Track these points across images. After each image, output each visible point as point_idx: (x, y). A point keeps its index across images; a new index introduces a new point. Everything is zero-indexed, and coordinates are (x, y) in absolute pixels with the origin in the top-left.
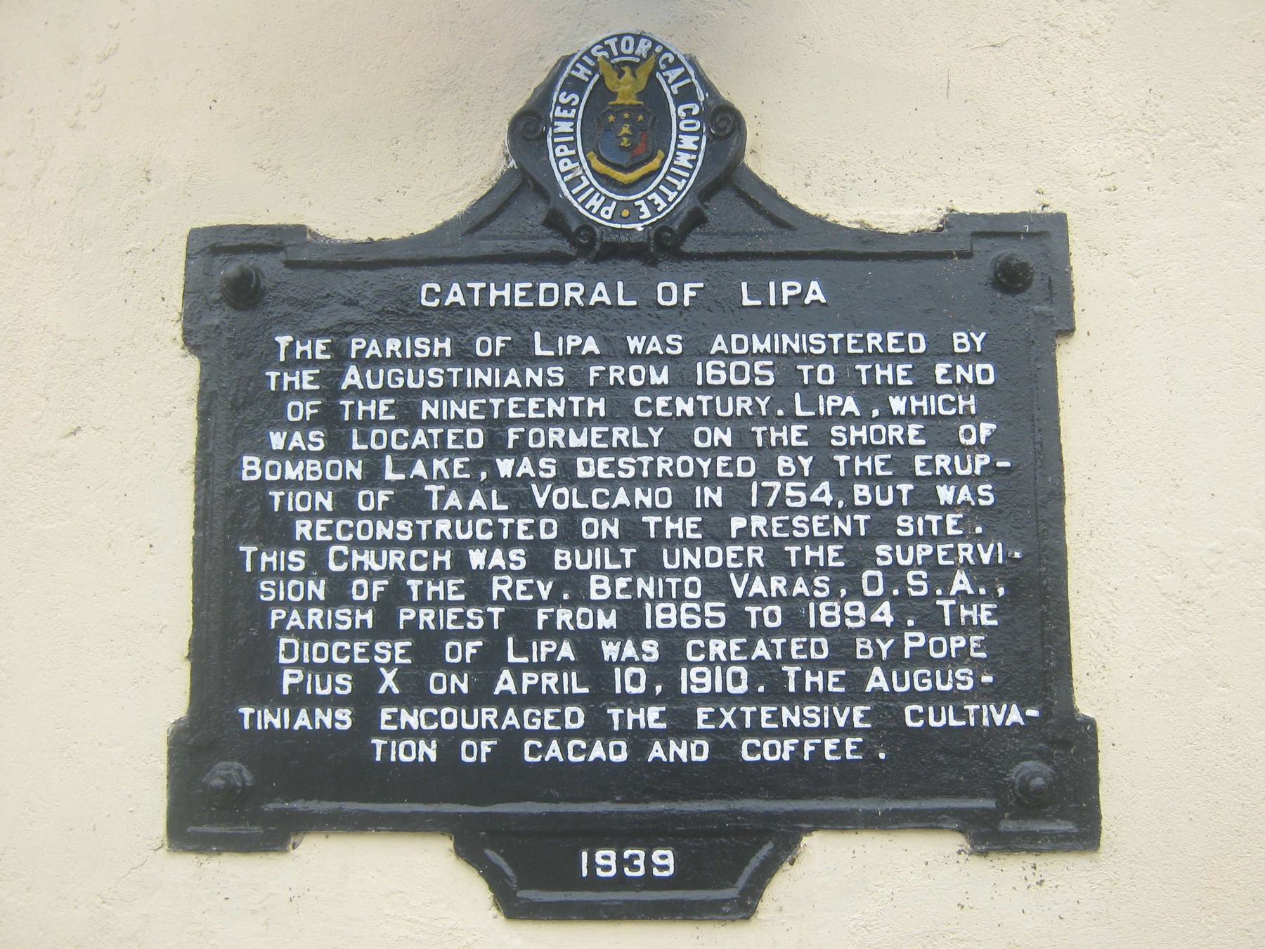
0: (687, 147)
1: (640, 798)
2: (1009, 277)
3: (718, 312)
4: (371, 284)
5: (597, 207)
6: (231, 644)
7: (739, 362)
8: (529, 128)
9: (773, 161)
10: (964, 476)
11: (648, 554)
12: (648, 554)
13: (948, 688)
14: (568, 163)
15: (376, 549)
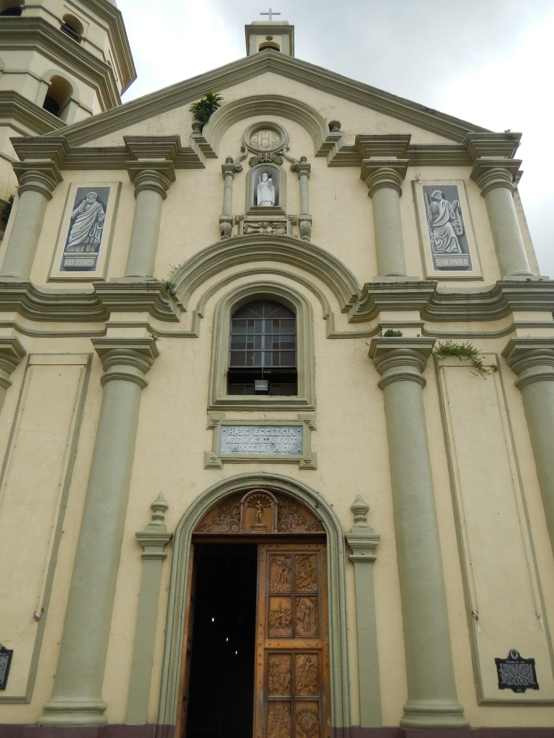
0: (517, 655)
3: (519, 663)
4: (503, 661)
5: (513, 658)
6: (500, 679)
7: (521, 665)
8: (510, 654)
9: (521, 655)
11: (518, 675)
12: (518, 675)
14: (512, 656)
15: (506, 675)
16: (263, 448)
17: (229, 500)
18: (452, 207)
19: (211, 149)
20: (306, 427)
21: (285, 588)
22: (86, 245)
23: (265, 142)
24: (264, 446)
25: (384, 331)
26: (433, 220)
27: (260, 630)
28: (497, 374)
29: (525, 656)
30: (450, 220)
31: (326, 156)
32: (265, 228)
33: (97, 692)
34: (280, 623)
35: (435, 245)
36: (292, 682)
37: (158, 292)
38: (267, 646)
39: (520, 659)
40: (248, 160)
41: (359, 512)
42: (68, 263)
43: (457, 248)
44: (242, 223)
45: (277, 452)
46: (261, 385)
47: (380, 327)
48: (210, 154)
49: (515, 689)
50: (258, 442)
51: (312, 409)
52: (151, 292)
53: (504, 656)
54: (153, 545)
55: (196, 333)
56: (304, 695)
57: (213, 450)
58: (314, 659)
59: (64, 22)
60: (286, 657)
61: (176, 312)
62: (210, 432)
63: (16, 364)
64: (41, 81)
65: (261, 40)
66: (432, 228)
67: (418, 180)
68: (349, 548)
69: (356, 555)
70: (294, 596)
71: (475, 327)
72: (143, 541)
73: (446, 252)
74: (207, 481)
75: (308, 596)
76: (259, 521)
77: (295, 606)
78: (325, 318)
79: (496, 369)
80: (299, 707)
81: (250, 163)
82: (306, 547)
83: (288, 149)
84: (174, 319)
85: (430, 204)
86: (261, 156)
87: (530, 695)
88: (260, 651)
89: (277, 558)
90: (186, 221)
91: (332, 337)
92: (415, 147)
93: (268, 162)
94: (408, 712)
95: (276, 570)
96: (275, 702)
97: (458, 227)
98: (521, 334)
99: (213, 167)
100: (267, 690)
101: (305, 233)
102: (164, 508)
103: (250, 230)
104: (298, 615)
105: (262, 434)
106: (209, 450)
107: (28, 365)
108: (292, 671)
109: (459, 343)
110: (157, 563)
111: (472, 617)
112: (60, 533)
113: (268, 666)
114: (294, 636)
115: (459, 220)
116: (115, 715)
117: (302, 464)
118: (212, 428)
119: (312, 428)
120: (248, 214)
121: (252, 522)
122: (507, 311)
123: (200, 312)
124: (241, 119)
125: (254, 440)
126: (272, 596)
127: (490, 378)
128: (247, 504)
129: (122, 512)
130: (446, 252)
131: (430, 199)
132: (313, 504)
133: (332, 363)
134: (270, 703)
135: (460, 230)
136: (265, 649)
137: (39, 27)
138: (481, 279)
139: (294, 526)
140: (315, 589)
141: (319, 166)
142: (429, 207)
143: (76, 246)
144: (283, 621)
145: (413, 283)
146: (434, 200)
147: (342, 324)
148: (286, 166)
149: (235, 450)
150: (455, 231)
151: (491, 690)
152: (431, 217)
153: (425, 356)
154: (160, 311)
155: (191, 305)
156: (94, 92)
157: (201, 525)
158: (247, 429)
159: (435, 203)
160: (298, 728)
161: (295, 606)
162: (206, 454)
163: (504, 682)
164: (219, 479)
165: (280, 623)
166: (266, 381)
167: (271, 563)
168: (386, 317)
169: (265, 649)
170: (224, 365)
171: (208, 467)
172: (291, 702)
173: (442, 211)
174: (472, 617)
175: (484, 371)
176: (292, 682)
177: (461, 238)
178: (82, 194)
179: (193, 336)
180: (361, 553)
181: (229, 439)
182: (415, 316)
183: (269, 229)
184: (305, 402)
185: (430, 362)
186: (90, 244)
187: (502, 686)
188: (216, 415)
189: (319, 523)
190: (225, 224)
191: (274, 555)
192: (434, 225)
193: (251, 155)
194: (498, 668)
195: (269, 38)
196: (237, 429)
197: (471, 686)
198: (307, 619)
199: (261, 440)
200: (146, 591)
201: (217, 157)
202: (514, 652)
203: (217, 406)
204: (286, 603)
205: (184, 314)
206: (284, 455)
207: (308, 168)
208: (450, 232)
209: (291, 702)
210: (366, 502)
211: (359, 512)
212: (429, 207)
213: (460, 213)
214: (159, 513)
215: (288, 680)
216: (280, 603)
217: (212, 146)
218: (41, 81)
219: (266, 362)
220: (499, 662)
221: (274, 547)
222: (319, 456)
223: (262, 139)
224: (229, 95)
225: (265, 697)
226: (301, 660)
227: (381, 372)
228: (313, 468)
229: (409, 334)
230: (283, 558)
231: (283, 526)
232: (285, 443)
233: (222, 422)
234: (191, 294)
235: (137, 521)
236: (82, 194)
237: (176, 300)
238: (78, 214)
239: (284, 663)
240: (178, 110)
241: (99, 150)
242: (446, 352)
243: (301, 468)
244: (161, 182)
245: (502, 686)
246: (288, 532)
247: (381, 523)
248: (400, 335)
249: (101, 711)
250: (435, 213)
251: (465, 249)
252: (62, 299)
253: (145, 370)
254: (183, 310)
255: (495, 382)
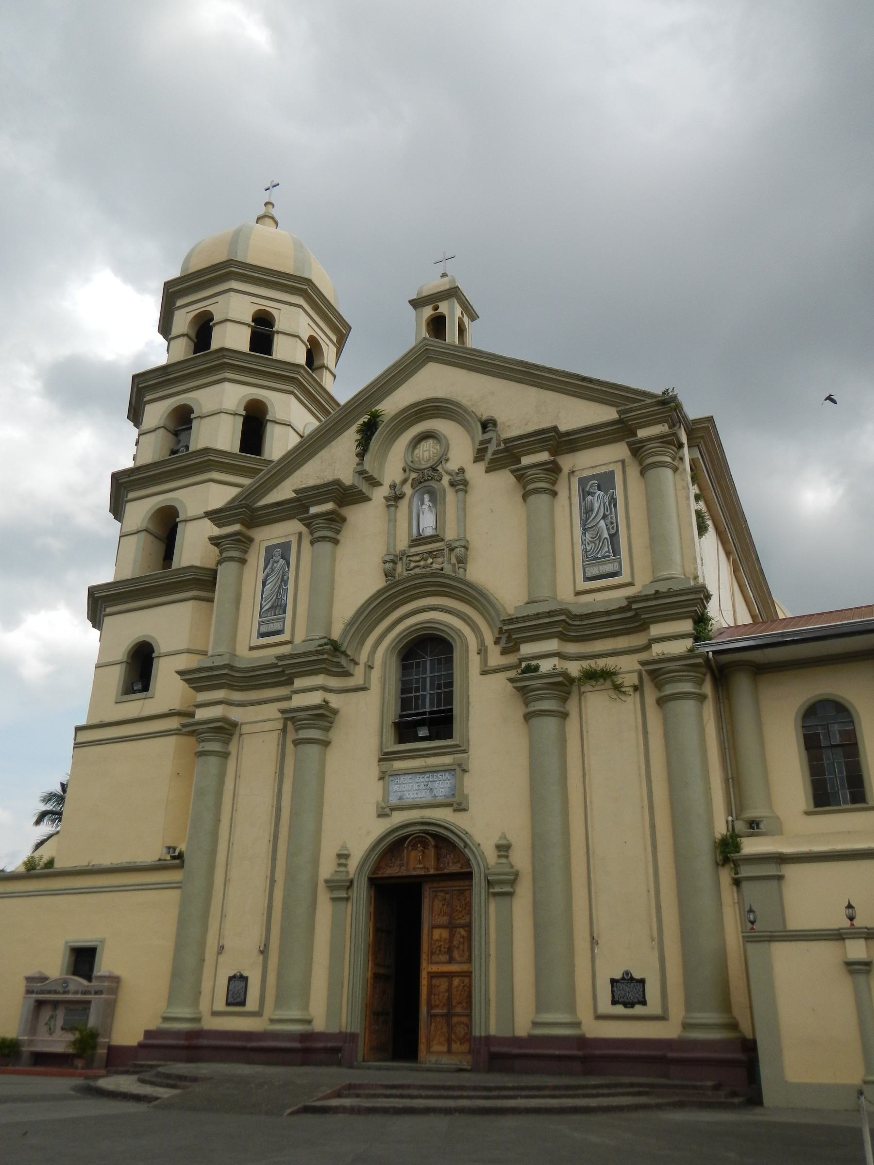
1: (629, 1003)
2: (642, 981)
6: (613, 996)
10: (641, 990)
13: (641, 999)
16: (423, 794)
17: (394, 846)
18: (606, 500)
19: (364, 494)
20: (458, 770)
21: (444, 920)
22: (276, 607)
23: (426, 454)
24: (424, 792)
25: (524, 665)
26: (587, 519)
27: (424, 957)
28: (638, 694)
29: (637, 976)
30: (604, 517)
31: (483, 460)
32: (426, 560)
33: (306, 1006)
34: (440, 951)
35: (586, 552)
36: (449, 999)
37: (325, 656)
38: (430, 970)
39: (632, 979)
40: (410, 481)
41: (504, 849)
42: (264, 629)
43: (608, 551)
44: (404, 558)
45: (435, 796)
46: (423, 732)
47: (521, 660)
48: (375, 483)
49: (626, 1005)
50: (419, 790)
51: (465, 751)
52: (320, 657)
53: (618, 976)
54: (340, 887)
55: (367, 686)
56: (458, 1010)
57: (383, 800)
58: (466, 980)
59: (253, 324)
60: (445, 979)
61: (350, 667)
62: (381, 782)
63: (232, 735)
64: (235, 414)
65: (428, 312)
66: (585, 530)
67: (573, 472)
68: (490, 884)
69: (497, 889)
70: (451, 927)
71: (622, 642)
72: (332, 885)
73: (597, 558)
74: (379, 828)
75: (462, 926)
76: (420, 863)
77: (452, 936)
78: (478, 653)
79: (636, 688)
80: (455, 1020)
81: (413, 486)
82: (461, 883)
83: (447, 460)
84: (348, 674)
85: (584, 499)
86: (421, 475)
87: (638, 1010)
88: (424, 975)
89: (439, 894)
90: (358, 565)
91: (484, 673)
92: (568, 434)
93: (428, 480)
94: (535, 1024)
95: (438, 904)
96: (436, 1015)
97: (612, 523)
98: (658, 649)
99: (379, 495)
100: (430, 1006)
101: (462, 561)
102: (347, 856)
103: (413, 565)
104: (455, 943)
105: (422, 780)
106: (380, 799)
107: (241, 735)
108: (449, 989)
109: (601, 664)
110: (342, 905)
111: (594, 941)
112: (273, 882)
113: (431, 987)
114: (451, 961)
115: (613, 515)
116: (319, 1025)
117: (455, 806)
118: (381, 779)
119: (465, 771)
120: (410, 546)
121: (415, 864)
122: (644, 627)
123: (370, 664)
124: (403, 432)
125: (415, 787)
126: (434, 927)
127: (630, 700)
128: (410, 848)
129: (315, 861)
130: (597, 558)
131: (585, 493)
132: (462, 845)
133: (485, 700)
134: (432, 1016)
135: (613, 528)
136: (429, 973)
137: (224, 357)
138: (631, 584)
139: (450, 864)
140: (468, 920)
141: (476, 473)
142: (583, 504)
143: (267, 610)
144: (442, 949)
145: (543, 613)
146: (589, 493)
147: (495, 658)
148: (446, 480)
149: (401, 798)
150: (608, 529)
151: (605, 1006)
152: (584, 516)
153: (564, 687)
154: (334, 669)
155: (363, 657)
156: (292, 397)
157: (377, 867)
158: (410, 776)
159: (590, 497)
160: (453, 1036)
161: (452, 936)
162: (378, 803)
163: (616, 998)
164: (389, 826)
165: (440, 951)
166: (426, 728)
167: (433, 899)
168: (527, 649)
169: (429, 973)
170: (393, 713)
171: (380, 816)
172: (448, 1016)
173: (596, 506)
174: (594, 941)
175: (624, 693)
176: (449, 999)
177: (614, 537)
178: (269, 550)
179: (364, 689)
180: (503, 887)
181: (396, 788)
182: (553, 645)
183: (430, 561)
184: (457, 746)
185: (575, 689)
186: (278, 607)
187: (614, 1002)
188: (386, 765)
189: (468, 863)
190: (388, 565)
191: (436, 891)
192: (587, 526)
193: (414, 475)
194: (612, 986)
195: (436, 308)
196: (402, 777)
197: (590, 1003)
198: (461, 946)
199: (422, 786)
200: (336, 926)
201: (382, 485)
202: (627, 973)
203: (386, 757)
204: (445, 933)
205: (357, 667)
206: (440, 799)
207: (465, 483)
208: (602, 531)
209: (448, 1016)
210: (512, 838)
211: (504, 849)
212: (583, 504)
213: (615, 506)
214: (343, 861)
215: (446, 998)
216: (441, 934)
217: (375, 476)
218: (235, 414)
219: (432, 705)
220: (613, 981)
221: (435, 885)
222: (470, 797)
223: (424, 451)
224: (390, 406)
225: (428, 1012)
226: (456, 981)
227: (527, 705)
228: (465, 810)
229: (546, 666)
230: (442, 894)
231: (442, 865)
232: (442, 787)
233: (389, 773)
234: (362, 645)
235: (327, 869)
236: (269, 550)
237: (347, 656)
238: (268, 575)
239: (443, 984)
240: (346, 434)
241: (278, 504)
242: (591, 676)
243: (455, 811)
244: (330, 529)
245: (614, 1002)
246: (446, 871)
247: (521, 859)
248: (536, 668)
249: (309, 1022)
250: (587, 511)
251: (616, 552)
252: (258, 670)
253: (327, 729)
254: (356, 663)
255: (635, 704)
